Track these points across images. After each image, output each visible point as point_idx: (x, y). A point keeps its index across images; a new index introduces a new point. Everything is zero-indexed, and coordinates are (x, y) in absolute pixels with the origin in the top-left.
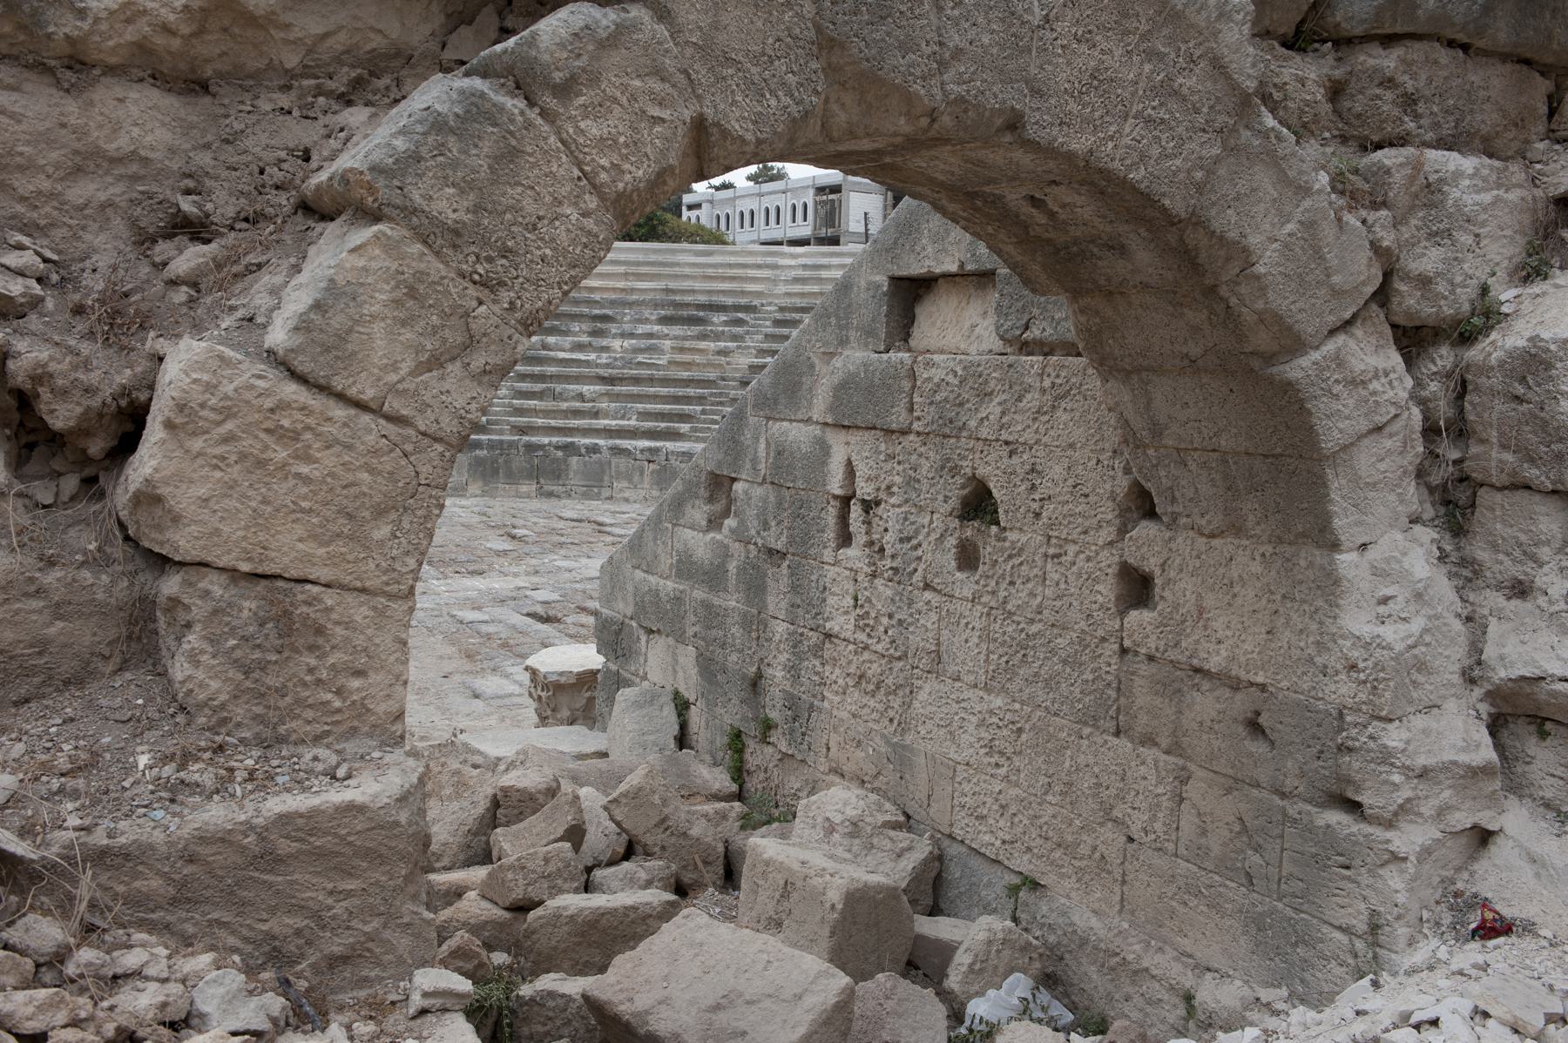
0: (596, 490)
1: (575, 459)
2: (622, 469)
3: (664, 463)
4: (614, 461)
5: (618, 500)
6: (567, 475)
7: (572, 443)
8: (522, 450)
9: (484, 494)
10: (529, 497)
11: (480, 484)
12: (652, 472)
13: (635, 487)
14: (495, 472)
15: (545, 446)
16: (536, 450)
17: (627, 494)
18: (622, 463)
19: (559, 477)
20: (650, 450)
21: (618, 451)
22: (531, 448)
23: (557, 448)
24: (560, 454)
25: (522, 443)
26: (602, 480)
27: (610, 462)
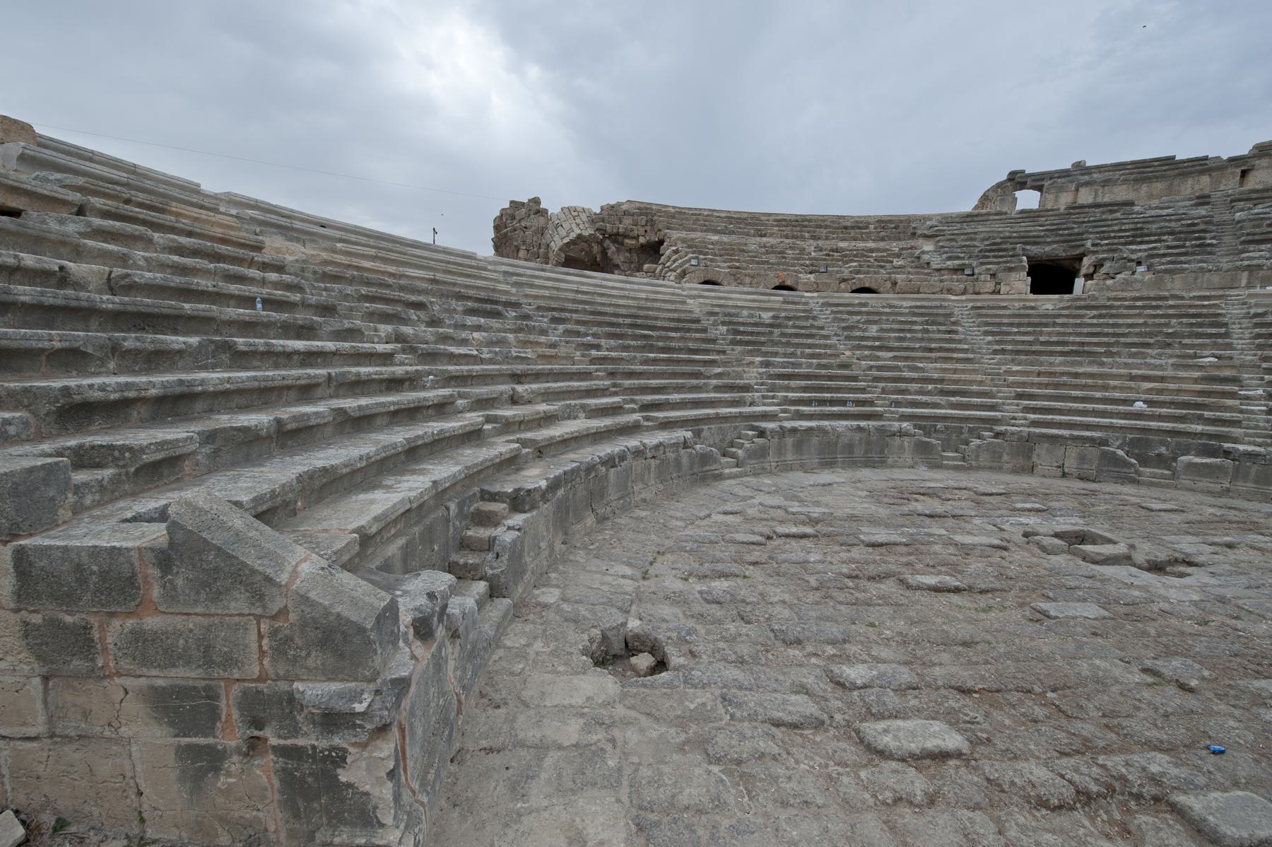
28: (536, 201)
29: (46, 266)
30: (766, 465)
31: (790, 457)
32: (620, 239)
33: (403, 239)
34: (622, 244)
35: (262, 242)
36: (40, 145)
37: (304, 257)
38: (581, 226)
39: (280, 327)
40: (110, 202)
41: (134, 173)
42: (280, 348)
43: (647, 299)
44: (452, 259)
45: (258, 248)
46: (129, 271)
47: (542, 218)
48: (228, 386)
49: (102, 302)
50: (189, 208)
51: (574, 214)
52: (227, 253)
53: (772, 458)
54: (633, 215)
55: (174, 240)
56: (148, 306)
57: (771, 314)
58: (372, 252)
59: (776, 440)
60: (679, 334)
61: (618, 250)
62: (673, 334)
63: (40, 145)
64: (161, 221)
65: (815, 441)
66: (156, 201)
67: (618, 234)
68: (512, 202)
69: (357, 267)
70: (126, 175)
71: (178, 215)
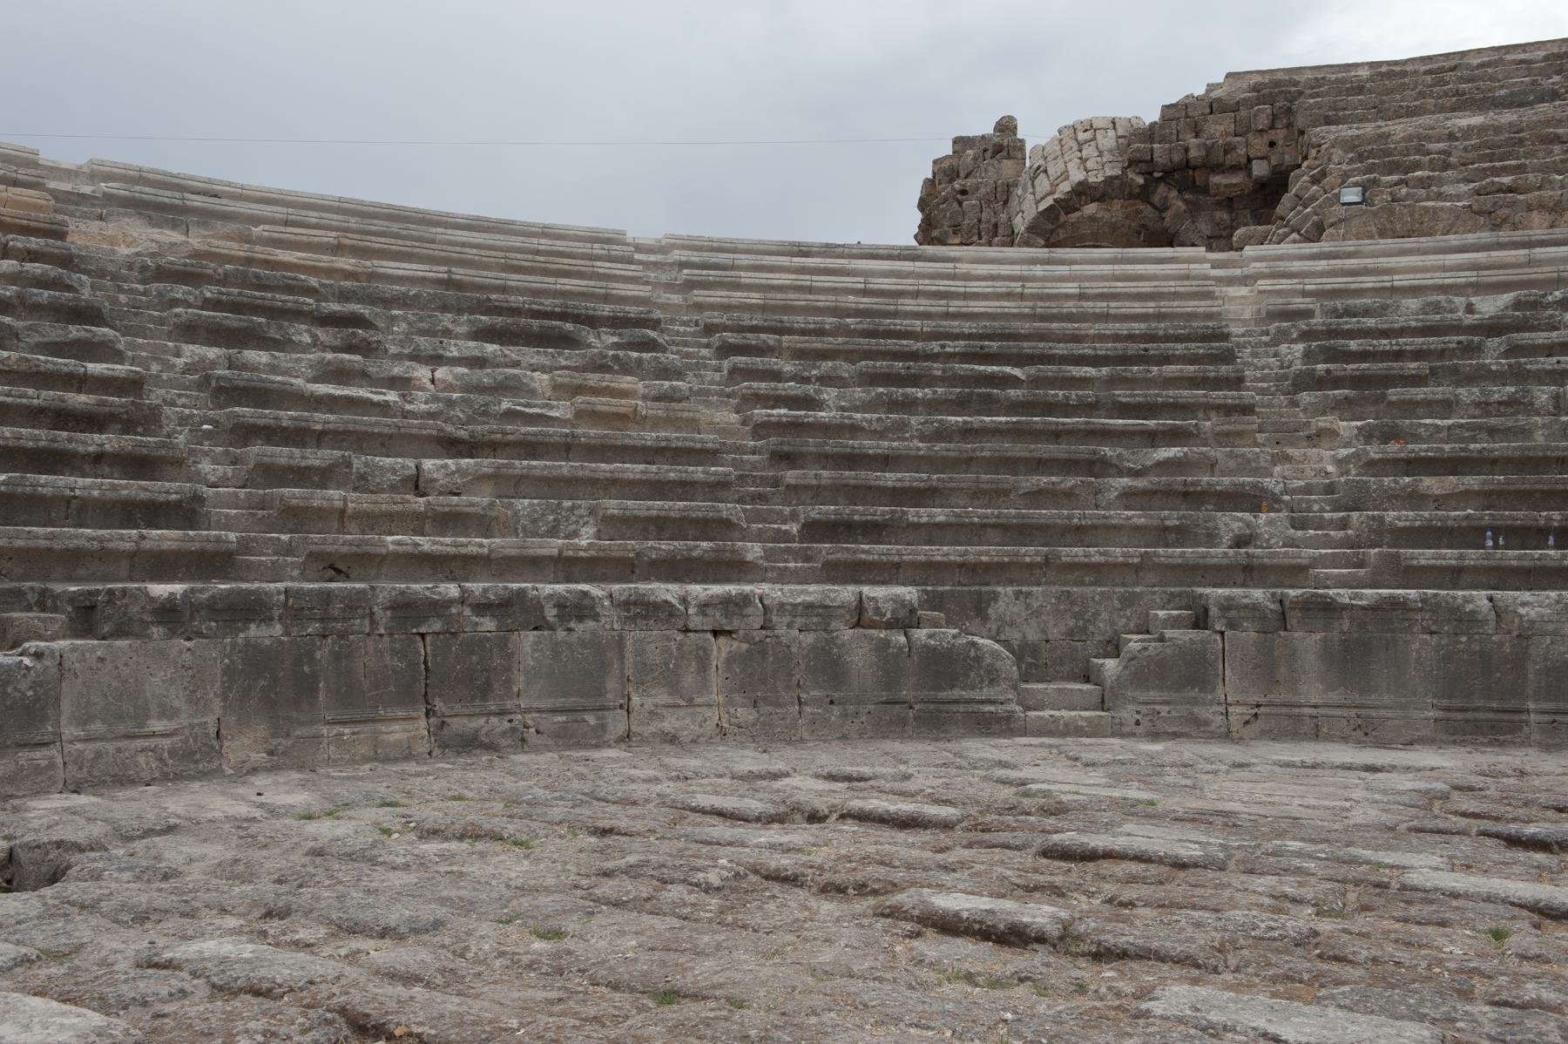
0: (591, 719)
1: (530, 637)
2: (654, 655)
3: (759, 635)
4: (632, 636)
5: (644, 740)
6: (508, 683)
7: (521, 593)
8: (383, 617)
9: (277, 762)
10: (409, 757)
11: (262, 729)
12: (729, 661)
13: (691, 703)
14: (306, 688)
15: (451, 602)
16: (423, 619)
17: (670, 723)
18: (652, 641)
19: (485, 691)
20: (726, 602)
21: (645, 611)
22: (407, 611)
23: (482, 608)
24: (488, 624)
25: (382, 597)
26: (600, 692)
27: (620, 643)
28: (1006, 126)
30: (1203, 713)
31: (1313, 692)
32: (1199, 177)
33: (448, 215)
34: (1205, 189)
38: (1089, 164)
43: (1082, 297)
44: (560, 245)
47: (1008, 163)
51: (1082, 136)
53: (1233, 686)
54: (1236, 107)
57: (1508, 298)
59: (1248, 635)
60: (1105, 371)
61: (1194, 209)
62: (1090, 371)
65: (1420, 645)
67: (1187, 165)
68: (956, 141)
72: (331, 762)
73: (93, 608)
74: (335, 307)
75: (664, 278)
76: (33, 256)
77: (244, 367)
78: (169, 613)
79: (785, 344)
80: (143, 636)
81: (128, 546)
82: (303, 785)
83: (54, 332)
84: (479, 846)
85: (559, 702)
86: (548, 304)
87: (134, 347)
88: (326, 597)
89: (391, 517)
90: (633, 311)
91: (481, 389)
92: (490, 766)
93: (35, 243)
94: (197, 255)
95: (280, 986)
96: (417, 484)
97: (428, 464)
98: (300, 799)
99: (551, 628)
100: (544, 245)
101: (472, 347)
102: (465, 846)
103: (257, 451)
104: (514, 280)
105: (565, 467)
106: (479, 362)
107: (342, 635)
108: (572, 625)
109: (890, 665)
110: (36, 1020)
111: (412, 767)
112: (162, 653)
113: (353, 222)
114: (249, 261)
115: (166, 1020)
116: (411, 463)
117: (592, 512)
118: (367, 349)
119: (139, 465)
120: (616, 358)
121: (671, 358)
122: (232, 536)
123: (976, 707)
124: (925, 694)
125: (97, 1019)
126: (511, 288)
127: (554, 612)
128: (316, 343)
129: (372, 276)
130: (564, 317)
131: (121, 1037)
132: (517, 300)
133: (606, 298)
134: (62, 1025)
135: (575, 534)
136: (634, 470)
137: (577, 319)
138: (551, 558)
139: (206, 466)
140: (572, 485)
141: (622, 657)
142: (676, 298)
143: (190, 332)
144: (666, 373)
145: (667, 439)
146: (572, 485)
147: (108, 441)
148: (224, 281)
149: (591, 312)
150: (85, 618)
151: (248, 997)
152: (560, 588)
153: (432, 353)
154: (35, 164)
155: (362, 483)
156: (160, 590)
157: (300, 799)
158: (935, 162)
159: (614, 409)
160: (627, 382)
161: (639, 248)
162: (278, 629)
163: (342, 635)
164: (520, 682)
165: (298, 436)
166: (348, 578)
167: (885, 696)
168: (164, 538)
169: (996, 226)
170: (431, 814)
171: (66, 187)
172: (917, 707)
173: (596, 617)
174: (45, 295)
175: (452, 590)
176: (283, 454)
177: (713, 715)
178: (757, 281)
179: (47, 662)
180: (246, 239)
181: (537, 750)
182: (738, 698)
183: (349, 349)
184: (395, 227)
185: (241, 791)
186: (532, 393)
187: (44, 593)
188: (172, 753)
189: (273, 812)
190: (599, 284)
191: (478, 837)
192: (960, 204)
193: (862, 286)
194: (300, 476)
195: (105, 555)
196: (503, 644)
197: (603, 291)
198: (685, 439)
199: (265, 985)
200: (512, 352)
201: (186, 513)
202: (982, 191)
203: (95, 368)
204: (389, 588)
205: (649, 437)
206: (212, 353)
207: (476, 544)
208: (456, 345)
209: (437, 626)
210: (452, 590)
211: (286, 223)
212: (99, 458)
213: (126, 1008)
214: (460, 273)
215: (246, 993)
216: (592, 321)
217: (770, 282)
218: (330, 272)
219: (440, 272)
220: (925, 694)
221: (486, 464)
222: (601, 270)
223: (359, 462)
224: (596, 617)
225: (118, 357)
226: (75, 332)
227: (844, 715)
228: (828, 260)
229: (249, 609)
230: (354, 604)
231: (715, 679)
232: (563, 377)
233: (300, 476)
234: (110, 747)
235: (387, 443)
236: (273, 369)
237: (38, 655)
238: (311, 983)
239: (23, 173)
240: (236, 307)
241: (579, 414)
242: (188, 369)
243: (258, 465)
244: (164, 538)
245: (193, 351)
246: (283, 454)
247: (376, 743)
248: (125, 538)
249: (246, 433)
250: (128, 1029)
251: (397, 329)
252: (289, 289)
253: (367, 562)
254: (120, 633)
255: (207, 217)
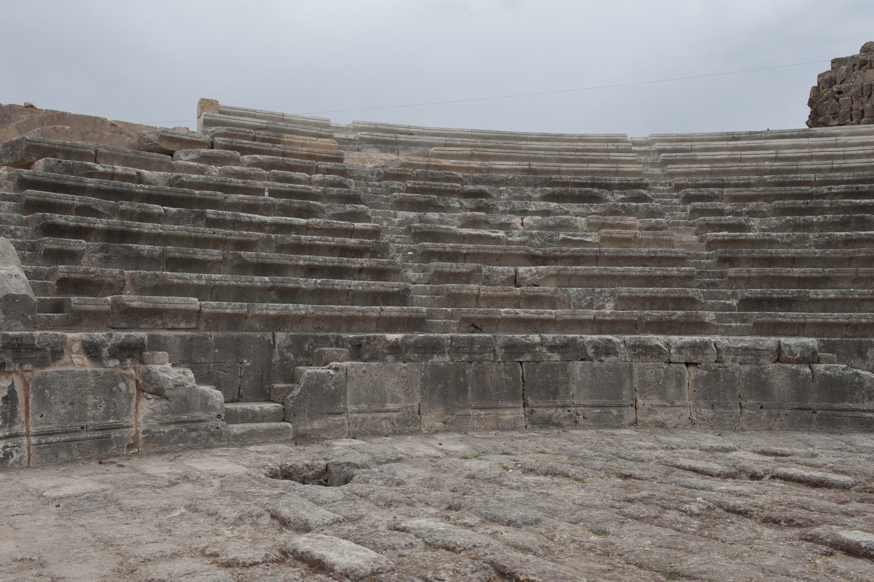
0: (614, 412)
1: (580, 364)
2: (650, 376)
3: (714, 366)
4: (637, 365)
5: (645, 425)
6: (567, 390)
7: (574, 339)
8: (500, 352)
9: (449, 427)
10: (515, 428)
11: (440, 411)
12: (696, 381)
13: (673, 405)
14: (462, 390)
15: (535, 345)
16: (521, 354)
17: (660, 416)
18: (649, 368)
19: (555, 394)
20: (693, 346)
21: (644, 351)
22: (513, 349)
23: (553, 348)
24: (556, 357)
25: (500, 342)
26: (619, 396)
27: (631, 368)
29: (128, 172)
33: (528, 134)
35: (342, 154)
36: (221, 112)
37: (383, 163)
39: (278, 210)
40: (227, 139)
41: (283, 120)
42: (247, 219)
44: (589, 146)
45: (340, 160)
46: (180, 174)
48: (161, 231)
49: (137, 188)
50: (297, 137)
52: (294, 164)
55: (255, 158)
56: (168, 191)
58: (467, 151)
63: (221, 112)
64: (261, 148)
66: (273, 135)
68: (833, 62)
69: (437, 166)
70: (266, 122)
71: (290, 143)
72: (474, 429)
73: (360, 346)
74: (471, 187)
75: (650, 159)
76: (329, 171)
77: (427, 221)
78: (395, 349)
79: (725, 194)
80: (383, 360)
81: (375, 314)
82: (461, 441)
83: (339, 208)
84: (556, 480)
85: (596, 401)
86: (584, 178)
87: (375, 214)
88: (471, 341)
89: (502, 298)
90: (632, 179)
91: (548, 228)
92: (558, 436)
93: (330, 165)
94: (403, 165)
95: (459, 546)
96: (515, 280)
97: (521, 269)
98: (461, 448)
99: (591, 360)
100: (581, 145)
101: (543, 205)
102: (548, 479)
103: (435, 265)
104: (565, 166)
105: (596, 269)
106: (546, 213)
107: (480, 362)
108: (603, 358)
109: (800, 386)
110: (346, 551)
111: (516, 434)
112: (392, 369)
113: (479, 142)
114: (428, 167)
115: (405, 558)
116: (512, 269)
117: (612, 294)
118: (488, 209)
119: (379, 273)
120: (623, 206)
121: (656, 205)
122: (424, 309)
123: (860, 414)
124: (824, 404)
125: (373, 554)
126: (563, 171)
127: (592, 350)
128: (462, 207)
129: (490, 170)
130: (592, 185)
131: (384, 565)
132: (566, 178)
133: (617, 173)
134: (357, 555)
135: (603, 307)
136: (636, 270)
137: (600, 186)
138: (590, 320)
139: (410, 273)
140: (600, 279)
141: (632, 377)
142: (657, 171)
143: (401, 205)
144: (652, 214)
145: (655, 252)
146: (600, 279)
147: (364, 262)
148: (416, 178)
149: (608, 182)
150: (357, 351)
151: (443, 550)
152: (595, 337)
153: (521, 209)
154: (329, 126)
155: (487, 280)
156: (391, 337)
157: (461, 448)
158: (819, 76)
159: (623, 236)
160: (630, 220)
161: (634, 144)
162: (447, 358)
163: (480, 362)
164: (574, 390)
165: (454, 256)
166: (481, 331)
167: (797, 405)
168: (392, 310)
169: (863, 112)
170: (529, 460)
171: (342, 136)
172: (819, 412)
173: (616, 354)
174: (335, 190)
175: (536, 338)
176: (447, 266)
177: (686, 412)
178: (707, 157)
179: (341, 373)
180: (426, 155)
181: (584, 428)
182: (701, 402)
183: (479, 209)
184: (500, 143)
185: (431, 442)
186: (576, 228)
187: (338, 338)
188: (398, 420)
189: (448, 454)
190: (612, 165)
191: (555, 475)
192: (837, 100)
193: (774, 155)
194: (456, 277)
195: (365, 319)
196: (564, 368)
197: (614, 169)
198: (666, 252)
199: (452, 545)
200: (564, 207)
201: (401, 297)
202: (853, 90)
203: (358, 225)
204: (503, 337)
205: (644, 251)
206: (412, 215)
207: (548, 313)
208: (534, 204)
209: (528, 357)
210: (536, 338)
211: (446, 145)
212: (361, 270)
213: (385, 550)
214: (535, 165)
215: (442, 548)
216: (609, 187)
217: (715, 157)
218: (467, 169)
219: (524, 165)
220: (824, 404)
221: (552, 269)
222: (613, 158)
223: (485, 269)
224: (616, 354)
225: (368, 219)
226: (349, 208)
227: (770, 416)
228: (751, 142)
229: (431, 348)
230: (486, 345)
231: (687, 391)
232: (593, 219)
233: (456, 277)
234: (369, 416)
235: (500, 259)
236: (441, 222)
237: (336, 369)
238: (475, 546)
239: (323, 132)
240: (423, 191)
241: (603, 240)
242: (401, 224)
243: (436, 272)
244: (392, 310)
245: (403, 214)
246: (447, 266)
247: (498, 421)
248: (374, 310)
249: (429, 256)
250: (387, 561)
251: (503, 197)
252: (448, 180)
253: (491, 323)
254: (373, 358)
255: (407, 145)
